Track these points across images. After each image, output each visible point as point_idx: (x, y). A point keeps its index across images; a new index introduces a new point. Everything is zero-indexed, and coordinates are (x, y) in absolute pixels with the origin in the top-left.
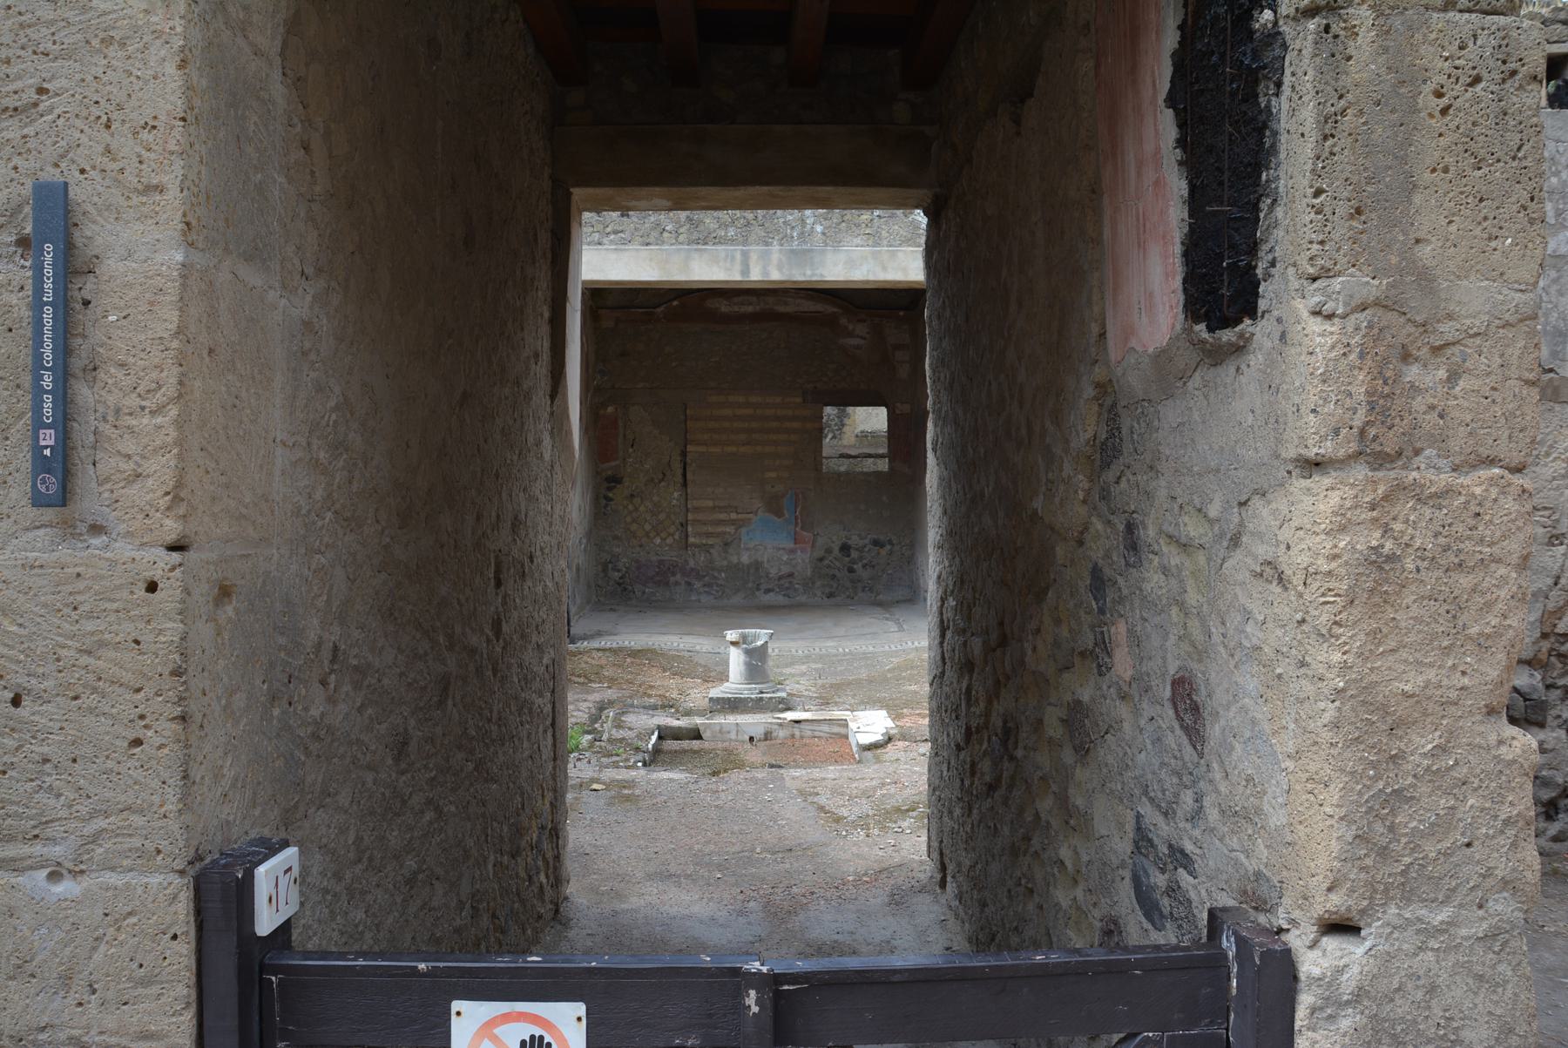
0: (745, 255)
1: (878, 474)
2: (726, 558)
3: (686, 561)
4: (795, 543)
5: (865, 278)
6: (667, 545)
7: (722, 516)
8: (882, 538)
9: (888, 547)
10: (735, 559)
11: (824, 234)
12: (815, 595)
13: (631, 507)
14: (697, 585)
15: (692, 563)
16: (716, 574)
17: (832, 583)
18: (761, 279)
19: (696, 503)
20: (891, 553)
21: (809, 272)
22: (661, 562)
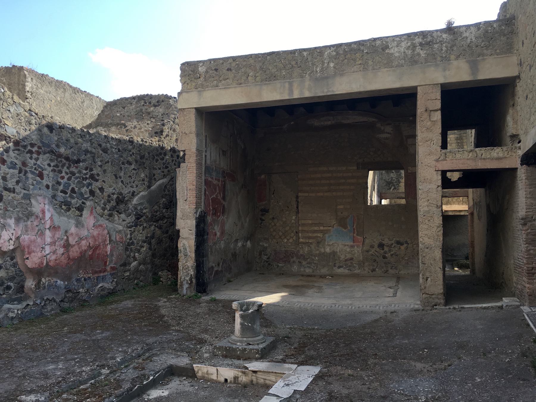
0: (291, 84)
1: (399, 205)
2: (318, 250)
3: (298, 251)
4: (354, 242)
5: (358, 90)
6: (290, 243)
7: (316, 228)
8: (402, 240)
9: (405, 245)
10: (322, 250)
11: (334, 67)
12: (364, 270)
13: (273, 224)
14: (304, 263)
15: (301, 252)
16: (313, 258)
17: (374, 263)
18: (299, 97)
19: (303, 222)
20: (407, 248)
21: (326, 90)
22: (286, 251)
